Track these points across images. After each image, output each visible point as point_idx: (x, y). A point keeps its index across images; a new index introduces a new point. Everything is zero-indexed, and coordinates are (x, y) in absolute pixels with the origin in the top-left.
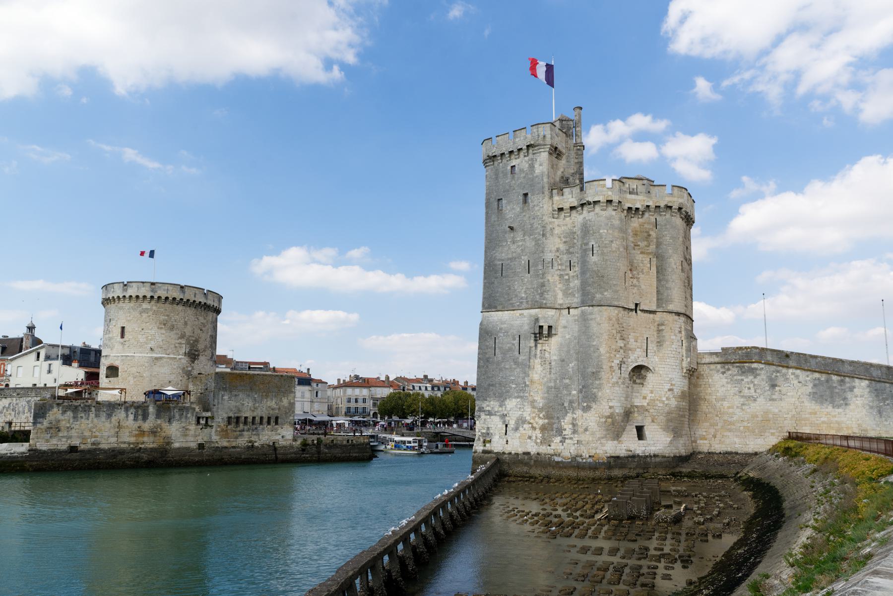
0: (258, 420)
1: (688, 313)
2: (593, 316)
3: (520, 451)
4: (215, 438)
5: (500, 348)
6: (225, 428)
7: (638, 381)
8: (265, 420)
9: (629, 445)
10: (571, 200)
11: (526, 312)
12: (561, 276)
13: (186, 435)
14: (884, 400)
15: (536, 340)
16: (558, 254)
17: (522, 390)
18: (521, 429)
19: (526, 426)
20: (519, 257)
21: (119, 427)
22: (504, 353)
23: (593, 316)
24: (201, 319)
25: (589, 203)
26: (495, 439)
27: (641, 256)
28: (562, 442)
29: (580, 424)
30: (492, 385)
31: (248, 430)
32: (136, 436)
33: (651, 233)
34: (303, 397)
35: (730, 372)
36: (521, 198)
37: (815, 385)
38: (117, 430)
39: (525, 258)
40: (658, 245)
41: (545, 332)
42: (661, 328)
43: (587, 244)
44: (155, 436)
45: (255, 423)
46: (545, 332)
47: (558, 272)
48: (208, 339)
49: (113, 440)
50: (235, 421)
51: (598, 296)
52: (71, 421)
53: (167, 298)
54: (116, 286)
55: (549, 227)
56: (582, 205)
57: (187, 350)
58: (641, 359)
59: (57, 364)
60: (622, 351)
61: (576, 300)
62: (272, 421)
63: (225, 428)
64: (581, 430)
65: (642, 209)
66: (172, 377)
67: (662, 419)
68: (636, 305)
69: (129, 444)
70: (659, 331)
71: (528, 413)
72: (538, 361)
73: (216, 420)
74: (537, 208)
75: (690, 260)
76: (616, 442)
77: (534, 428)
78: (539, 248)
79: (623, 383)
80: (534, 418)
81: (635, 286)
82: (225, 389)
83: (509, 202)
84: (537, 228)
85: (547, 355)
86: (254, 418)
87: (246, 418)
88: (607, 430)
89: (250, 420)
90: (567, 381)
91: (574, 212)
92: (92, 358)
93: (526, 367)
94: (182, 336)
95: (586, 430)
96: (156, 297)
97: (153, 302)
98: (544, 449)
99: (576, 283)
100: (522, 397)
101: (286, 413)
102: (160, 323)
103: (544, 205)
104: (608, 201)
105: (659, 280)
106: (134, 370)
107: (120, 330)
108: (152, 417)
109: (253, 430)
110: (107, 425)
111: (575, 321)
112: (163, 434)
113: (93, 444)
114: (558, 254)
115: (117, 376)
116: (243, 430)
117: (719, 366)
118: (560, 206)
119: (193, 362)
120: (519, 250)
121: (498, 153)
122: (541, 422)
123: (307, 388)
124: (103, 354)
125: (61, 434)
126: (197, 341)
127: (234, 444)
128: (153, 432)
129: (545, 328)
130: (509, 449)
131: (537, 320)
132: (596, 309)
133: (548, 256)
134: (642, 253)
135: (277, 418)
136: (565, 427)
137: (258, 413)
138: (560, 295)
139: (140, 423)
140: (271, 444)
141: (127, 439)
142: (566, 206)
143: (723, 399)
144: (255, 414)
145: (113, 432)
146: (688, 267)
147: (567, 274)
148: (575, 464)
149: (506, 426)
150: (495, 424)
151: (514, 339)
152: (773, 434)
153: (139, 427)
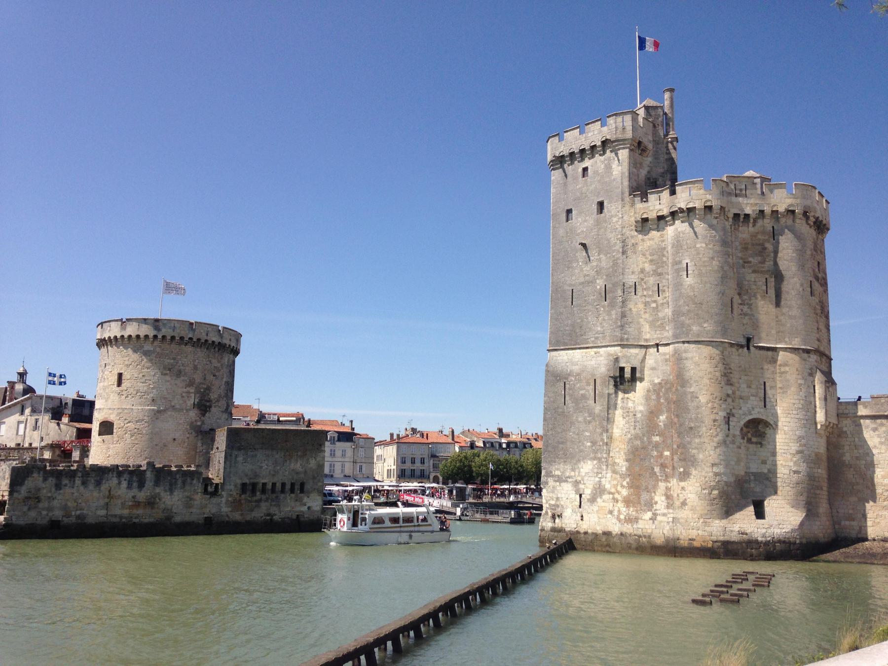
0: (279, 486)
1: (822, 349)
2: (689, 355)
3: (599, 529)
4: (225, 509)
5: (571, 396)
6: (238, 497)
7: (754, 440)
8: (288, 487)
11: (602, 351)
12: (646, 304)
13: (190, 507)
15: (616, 386)
16: (642, 276)
17: (600, 450)
18: (599, 500)
19: (606, 497)
21: (110, 496)
23: (689, 355)
24: (215, 363)
27: (754, 275)
28: (653, 519)
29: (675, 495)
30: (562, 443)
31: (267, 500)
32: (131, 507)
33: (767, 245)
34: (344, 455)
35: (884, 429)
36: (595, 207)
38: (107, 500)
39: (600, 283)
41: (628, 374)
43: (680, 262)
44: (153, 508)
45: (275, 491)
46: (628, 374)
47: (643, 299)
48: (223, 387)
49: (103, 512)
50: (249, 488)
52: (53, 490)
53: (173, 338)
54: (113, 324)
56: (673, 214)
57: (197, 400)
58: (756, 410)
59: (45, 418)
60: (729, 400)
61: (666, 334)
62: (297, 487)
63: (238, 497)
64: (677, 503)
65: (753, 216)
66: (177, 435)
68: (749, 340)
69: (121, 517)
72: (619, 413)
73: (227, 487)
75: (825, 279)
76: (724, 521)
77: (616, 501)
78: (616, 269)
79: (733, 442)
80: (615, 486)
81: (745, 315)
82: (239, 449)
83: (580, 213)
85: (630, 404)
86: (274, 484)
87: (264, 484)
88: (712, 504)
89: (269, 486)
90: (657, 439)
91: (662, 222)
92: (86, 412)
94: (191, 384)
96: (160, 337)
97: (156, 343)
98: (628, 529)
99: (668, 312)
100: (599, 459)
101: (314, 478)
102: (165, 368)
104: (705, 207)
106: (131, 426)
107: (116, 377)
108: (149, 484)
109: (272, 500)
110: (96, 494)
111: (666, 360)
112: (162, 506)
113: (78, 517)
114: (642, 276)
115: (112, 433)
116: (260, 500)
118: (645, 216)
119: (204, 415)
120: (593, 273)
121: (566, 153)
122: (625, 492)
123: (349, 444)
124: (97, 406)
125: (41, 505)
126: (208, 389)
127: (248, 518)
128: (151, 503)
130: (584, 527)
131: (617, 360)
134: (754, 272)
135: (302, 485)
136: (657, 498)
137: (278, 479)
138: (646, 328)
139: (135, 491)
140: (294, 517)
141: (118, 511)
142: (652, 215)
144: (275, 480)
145: (102, 502)
146: (821, 289)
147: (655, 302)
149: (581, 496)
151: (588, 384)
153: (134, 497)
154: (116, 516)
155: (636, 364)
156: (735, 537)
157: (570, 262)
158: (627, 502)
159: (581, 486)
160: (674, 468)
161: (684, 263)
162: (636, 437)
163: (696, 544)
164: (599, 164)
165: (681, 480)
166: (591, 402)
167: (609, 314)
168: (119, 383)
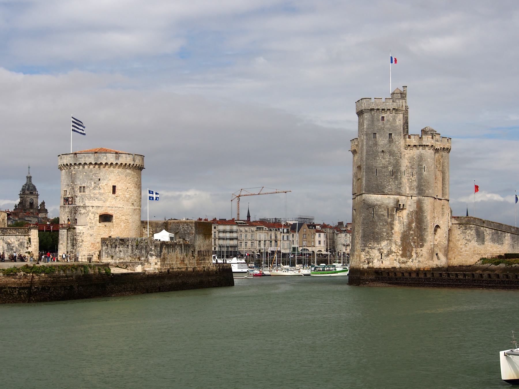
3: (390, 267)
5: (376, 214)
9: (435, 263)
10: (414, 142)
11: (391, 196)
12: (408, 179)
14: (515, 241)
17: (389, 237)
19: (393, 254)
20: (387, 167)
22: (379, 216)
25: (424, 146)
26: (375, 261)
36: (388, 135)
37: (492, 235)
39: (390, 168)
40: (443, 166)
42: (444, 207)
43: (422, 165)
51: (427, 191)
55: (403, 154)
56: (420, 145)
61: (415, 192)
67: (443, 250)
70: (443, 208)
71: (394, 248)
74: (397, 143)
83: (381, 136)
84: (397, 154)
85: (401, 219)
90: (412, 232)
93: (391, 226)
95: (422, 256)
98: (403, 266)
100: (390, 240)
103: (401, 142)
105: (443, 184)
117: (457, 225)
120: (387, 163)
122: (401, 252)
129: (402, 205)
130: (383, 266)
131: (398, 201)
132: (426, 198)
133: (403, 169)
138: (408, 189)
143: (459, 240)
148: (418, 271)
150: (375, 253)
152: (477, 257)
154: (178, 268)
155: (404, 203)
156: (435, 266)
157: (376, 156)
158: (403, 256)
159: (382, 250)
160: (418, 243)
161: (424, 165)
162: (404, 232)
163: (425, 269)
164: (390, 117)
165: (421, 247)
166: (386, 217)
167: (394, 182)
168: (114, 192)
